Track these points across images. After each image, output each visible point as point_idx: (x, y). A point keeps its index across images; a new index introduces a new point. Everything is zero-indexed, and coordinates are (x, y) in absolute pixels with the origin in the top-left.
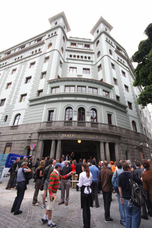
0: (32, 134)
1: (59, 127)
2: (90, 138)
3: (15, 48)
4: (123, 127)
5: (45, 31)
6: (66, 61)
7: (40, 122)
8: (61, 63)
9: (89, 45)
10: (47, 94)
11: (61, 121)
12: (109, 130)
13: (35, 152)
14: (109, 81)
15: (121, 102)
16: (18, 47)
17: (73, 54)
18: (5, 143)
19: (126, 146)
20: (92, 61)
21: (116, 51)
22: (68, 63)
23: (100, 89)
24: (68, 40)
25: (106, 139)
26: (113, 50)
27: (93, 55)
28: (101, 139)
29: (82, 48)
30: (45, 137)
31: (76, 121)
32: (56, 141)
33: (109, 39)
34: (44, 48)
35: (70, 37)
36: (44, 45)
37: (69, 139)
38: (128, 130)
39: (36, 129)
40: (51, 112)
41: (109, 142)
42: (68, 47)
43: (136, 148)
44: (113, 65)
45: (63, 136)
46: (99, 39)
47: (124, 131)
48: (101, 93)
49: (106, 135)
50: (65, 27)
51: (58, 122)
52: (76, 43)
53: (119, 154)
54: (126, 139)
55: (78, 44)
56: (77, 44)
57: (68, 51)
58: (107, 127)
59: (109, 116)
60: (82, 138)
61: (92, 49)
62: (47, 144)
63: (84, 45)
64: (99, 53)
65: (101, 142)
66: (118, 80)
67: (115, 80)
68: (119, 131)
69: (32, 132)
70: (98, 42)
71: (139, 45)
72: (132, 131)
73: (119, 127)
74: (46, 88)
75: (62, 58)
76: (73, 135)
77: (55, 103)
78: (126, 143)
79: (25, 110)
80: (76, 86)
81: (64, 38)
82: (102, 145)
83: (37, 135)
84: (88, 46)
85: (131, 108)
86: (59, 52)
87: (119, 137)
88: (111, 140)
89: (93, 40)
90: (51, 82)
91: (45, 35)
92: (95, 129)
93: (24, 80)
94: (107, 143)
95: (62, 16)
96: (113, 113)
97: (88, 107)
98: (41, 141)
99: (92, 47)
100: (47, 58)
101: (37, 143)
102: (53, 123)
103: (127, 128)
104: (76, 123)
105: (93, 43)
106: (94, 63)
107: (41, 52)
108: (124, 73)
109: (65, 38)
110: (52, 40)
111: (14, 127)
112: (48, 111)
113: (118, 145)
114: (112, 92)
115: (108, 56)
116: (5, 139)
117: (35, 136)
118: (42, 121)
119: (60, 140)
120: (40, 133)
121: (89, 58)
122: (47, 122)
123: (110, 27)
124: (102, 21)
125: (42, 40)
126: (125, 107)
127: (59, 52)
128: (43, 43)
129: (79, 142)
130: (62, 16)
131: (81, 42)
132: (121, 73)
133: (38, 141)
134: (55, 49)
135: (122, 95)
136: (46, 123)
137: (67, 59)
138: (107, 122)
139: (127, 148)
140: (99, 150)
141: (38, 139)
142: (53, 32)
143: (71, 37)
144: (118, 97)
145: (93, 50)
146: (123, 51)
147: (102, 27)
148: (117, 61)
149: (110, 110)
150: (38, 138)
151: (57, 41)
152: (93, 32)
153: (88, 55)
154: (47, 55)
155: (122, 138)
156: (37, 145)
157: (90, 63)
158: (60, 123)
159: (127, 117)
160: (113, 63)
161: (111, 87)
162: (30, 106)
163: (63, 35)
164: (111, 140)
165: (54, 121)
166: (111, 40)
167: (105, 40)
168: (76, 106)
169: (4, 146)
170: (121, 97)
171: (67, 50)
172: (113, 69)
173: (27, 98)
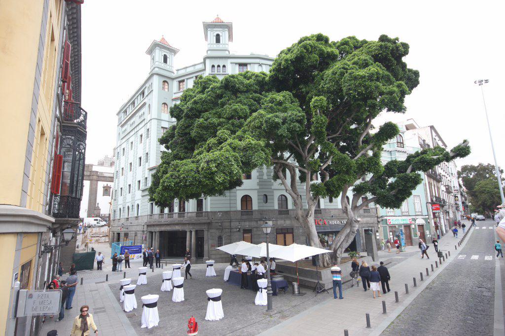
4: (217, 210)
5: (143, 82)
12: (195, 218)
18: (134, 232)
24: (173, 79)
25: (191, 228)
28: (187, 228)
35: (178, 70)
39: (145, 220)
43: (239, 231)
45: (158, 229)
47: (220, 215)
54: (220, 224)
58: (194, 215)
73: (211, 212)
82: (188, 234)
91: (146, 88)
92: (182, 219)
103: (228, 209)
111: (137, 218)
116: (134, 229)
128: (145, 104)
134: (153, 117)
162: (143, 196)
164: (198, 228)
169: (134, 235)
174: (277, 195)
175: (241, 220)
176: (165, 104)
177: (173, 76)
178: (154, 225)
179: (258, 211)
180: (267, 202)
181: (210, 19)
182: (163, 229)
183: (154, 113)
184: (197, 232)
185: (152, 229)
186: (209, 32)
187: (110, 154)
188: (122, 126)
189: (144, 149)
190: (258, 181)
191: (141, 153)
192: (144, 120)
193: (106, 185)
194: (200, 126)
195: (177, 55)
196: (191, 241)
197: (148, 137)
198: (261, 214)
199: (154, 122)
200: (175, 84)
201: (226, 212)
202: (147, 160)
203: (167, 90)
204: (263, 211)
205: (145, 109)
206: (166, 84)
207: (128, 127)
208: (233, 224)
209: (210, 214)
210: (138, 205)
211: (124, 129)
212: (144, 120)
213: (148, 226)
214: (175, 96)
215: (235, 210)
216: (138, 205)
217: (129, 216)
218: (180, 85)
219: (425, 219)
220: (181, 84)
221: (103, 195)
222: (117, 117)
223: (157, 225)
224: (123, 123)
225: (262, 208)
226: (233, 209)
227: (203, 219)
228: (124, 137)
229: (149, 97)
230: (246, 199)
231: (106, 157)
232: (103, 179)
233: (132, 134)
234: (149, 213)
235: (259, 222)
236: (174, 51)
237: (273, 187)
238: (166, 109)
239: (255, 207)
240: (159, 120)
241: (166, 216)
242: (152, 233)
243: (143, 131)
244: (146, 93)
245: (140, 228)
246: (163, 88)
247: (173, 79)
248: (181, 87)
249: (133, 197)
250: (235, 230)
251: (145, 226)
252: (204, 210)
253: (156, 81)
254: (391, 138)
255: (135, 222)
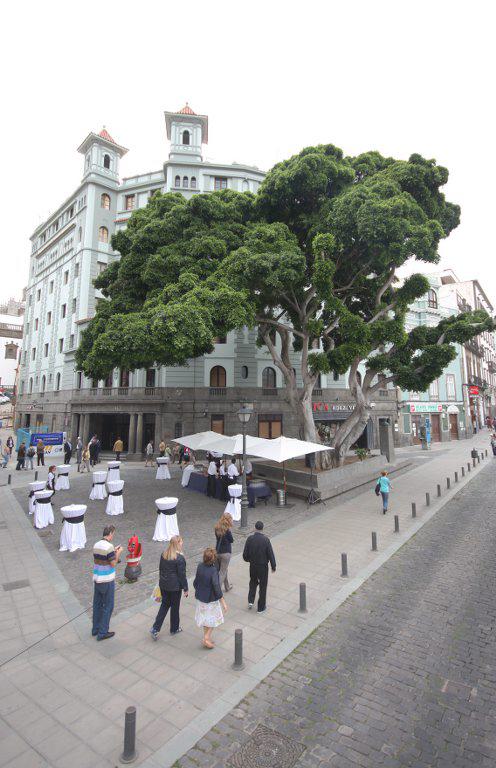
24: (118, 192)
28: (130, 411)
30: (75, 410)
35: (125, 180)
39: (70, 397)
43: (206, 416)
45: (88, 410)
58: (142, 391)
82: (132, 419)
103: (192, 385)
111: (57, 393)
116: (52, 409)
128: (73, 226)
134: (85, 246)
142: (81, 196)
162: (66, 362)
164: (147, 410)
173: (66, 348)
174: (261, 367)
175: (209, 401)
176: (103, 228)
177: (119, 187)
179: (234, 388)
180: (246, 376)
181: (175, 109)
182: (96, 410)
183: (87, 242)
184: (144, 415)
185: (79, 410)
186: (173, 128)
187: (19, 297)
188: (38, 257)
189: (71, 292)
190: (235, 346)
191: (65, 299)
192: (72, 250)
193: (10, 343)
194: (155, 266)
195: (124, 157)
196: (136, 428)
197: (76, 275)
198: (238, 394)
199: (87, 255)
200: (120, 200)
201: (190, 390)
202: (74, 309)
203: (107, 208)
204: (240, 389)
205: (74, 234)
206: (107, 198)
207: (47, 259)
208: (196, 406)
209: (165, 392)
210: (59, 375)
211: (41, 261)
212: (72, 250)
213: (72, 405)
214: (118, 218)
215: (201, 386)
216: (59, 375)
217: (46, 390)
218: (127, 202)
219: (459, 407)
220: (130, 200)
221: (6, 358)
222: (30, 243)
223: (86, 405)
224: (40, 252)
225: (240, 385)
226: (198, 385)
227: (155, 398)
228: (39, 272)
229: (80, 217)
230: (218, 372)
231: (12, 301)
232: (5, 333)
233: (52, 269)
234: (75, 387)
235: (234, 405)
236: (121, 152)
237: (257, 356)
238: (105, 235)
239: (230, 382)
240: (95, 251)
241: (99, 393)
242: (79, 416)
243: (69, 267)
244: (76, 211)
245: (61, 408)
246: (103, 205)
247: (118, 192)
248: (130, 204)
249: (52, 363)
250: (199, 415)
251: (69, 407)
252: (156, 385)
253: (91, 191)
254: (419, 297)
255: (53, 399)
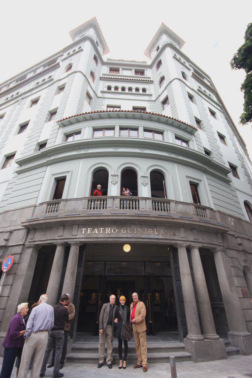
0: (11, 232)
1: (76, 212)
2: (152, 236)
3: (8, 83)
4: (228, 212)
5: (61, 49)
6: (100, 95)
7: (32, 202)
8: (89, 96)
9: (144, 70)
10: (56, 143)
11: (81, 199)
13: (11, 278)
14: (185, 118)
15: (215, 158)
16: (14, 81)
17: (113, 84)
19: (241, 257)
20: (151, 95)
21: (194, 76)
22: (103, 99)
23: (169, 133)
24: (103, 63)
26: (189, 74)
27: (151, 85)
28: (181, 238)
29: (130, 75)
30: (41, 238)
31: (117, 197)
32: (67, 248)
33: (178, 56)
34: (58, 74)
35: (108, 59)
36: (59, 69)
37: (99, 240)
38: (239, 219)
40: (60, 182)
41: (200, 245)
42: (103, 75)
44: (191, 97)
45: (83, 234)
46: (161, 58)
48: (169, 138)
49: (191, 228)
50: (98, 44)
51: (73, 202)
52: (119, 68)
53: (229, 277)
54: (239, 241)
55: (123, 69)
56: (121, 70)
57: (103, 80)
58: (191, 210)
59: (194, 186)
60: (130, 236)
61: (148, 76)
62: (44, 255)
63: (133, 71)
64: (162, 79)
65: (181, 246)
66: (203, 122)
67: (198, 122)
68: (219, 220)
69: (13, 228)
70: (160, 63)
71: (246, 32)
72: (246, 222)
73: (219, 212)
74: (54, 136)
75: (91, 87)
76: (108, 230)
77: (73, 161)
78: (241, 248)
79: (7, 183)
80: (117, 128)
81: (95, 58)
82: (182, 255)
83: (23, 233)
84: (140, 72)
85: (236, 175)
86: (85, 76)
87: (222, 233)
88: (206, 241)
89: (149, 62)
90: (63, 124)
93: (17, 128)
94: (194, 247)
95: (93, 24)
96: (201, 181)
97: (143, 168)
98: (29, 247)
99: (148, 73)
100: (61, 89)
101: (21, 254)
102: (62, 203)
104: (117, 201)
105: (150, 67)
106: (153, 98)
107: (53, 80)
108: (213, 113)
109: (97, 58)
110: (73, 60)
112: (53, 180)
113: (223, 253)
114: (194, 139)
115: (180, 80)
117: (18, 238)
118: (40, 201)
119: (76, 244)
120: (31, 228)
121: (144, 90)
122: (49, 204)
123: (180, 42)
124: (164, 31)
125: (57, 62)
126: (226, 172)
127: (85, 76)
128: (58, 66)
129: (127, 248)
130: (93, 24)
131: (127, 66)
132: (209, 113)
133: (23, 250)
135: (215, 149)
136: (46, 205)
137: (102, 92)
138: (190, 200)
139: (246, 261)
140: (177, 268)
141: (24, 245)
142: (76, 48)
143: (111, 60)
144: (208, 153)
145: (150, 78)
146: (206, 78)
147: (165, 39)
148: (197, 91)
149: (196, 175)
150: (25, 242)
151: (83, 60)
152: (150, 50)
153: (141, 86)
154: (61, 83)
155: (229, 237)
156: (20, 258)
157: (147, 98)
158: (79, 202)
159: (233, 193)
160: (192, 92)
161: (191, 131)
162: (19, 173)
163: (94, 53)
164: (206, 241)
165: (64, 200)
166: (182, 58)
167: (172, 56)
168: (115, 167)
170: (213, 151)
171: (101, 79)
172: (191, 102)
178: (64, 225)
